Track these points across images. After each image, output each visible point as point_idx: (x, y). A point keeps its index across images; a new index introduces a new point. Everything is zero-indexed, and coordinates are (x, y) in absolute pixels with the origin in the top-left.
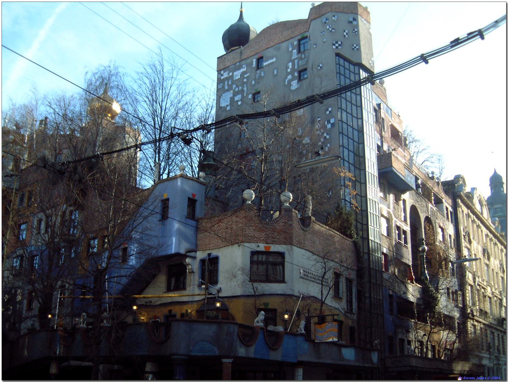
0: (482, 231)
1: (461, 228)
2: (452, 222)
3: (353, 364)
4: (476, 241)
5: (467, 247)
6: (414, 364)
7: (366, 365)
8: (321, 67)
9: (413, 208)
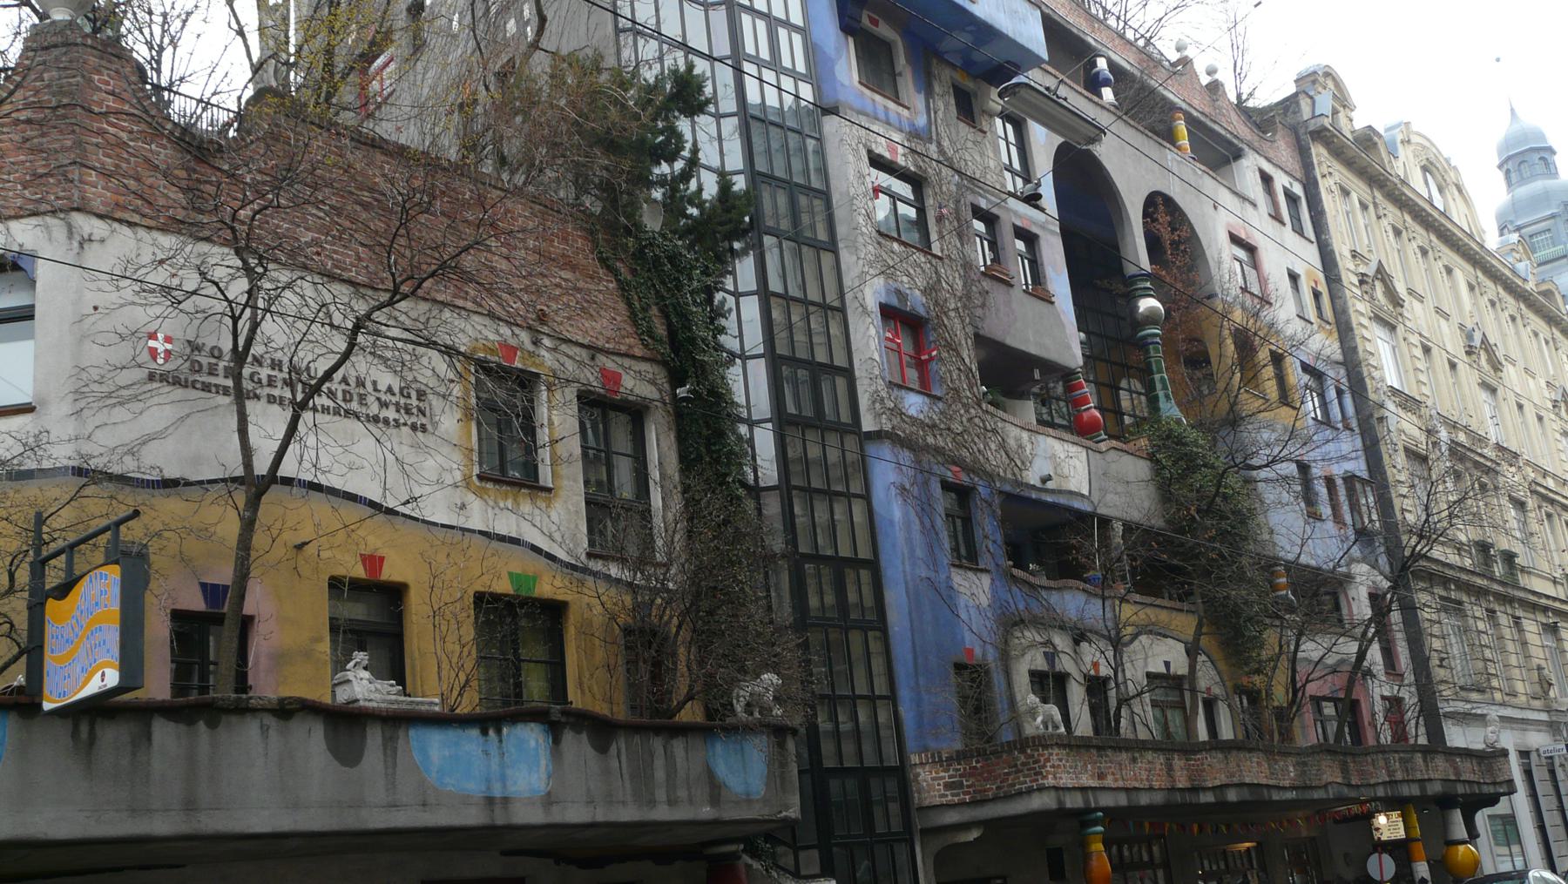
0: (1449, 271)
1: (1341, 248)
2: (1299, 231)
3: (532, 815)
4: (1421, 299)
5: (1378, 319)
6: (1066, 780)
7: (662, 813)
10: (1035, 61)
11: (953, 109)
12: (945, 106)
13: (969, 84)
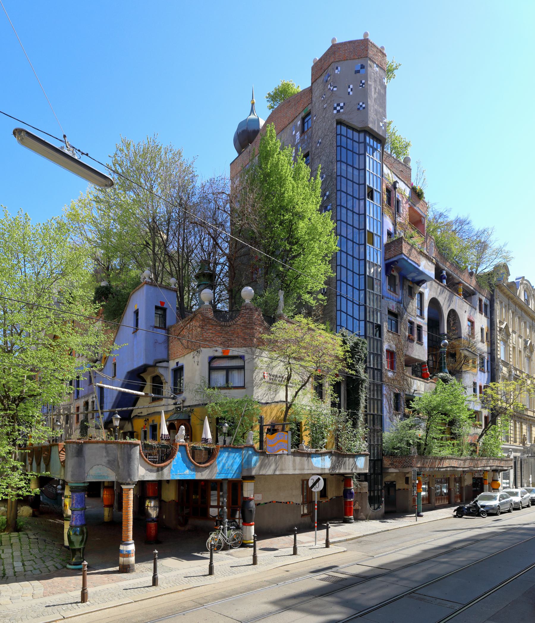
8: (320, 143)
9: (434, 302)
10: (430, 279)
11: (408, 293)
12: (406, 292)
13: (411, 285)
